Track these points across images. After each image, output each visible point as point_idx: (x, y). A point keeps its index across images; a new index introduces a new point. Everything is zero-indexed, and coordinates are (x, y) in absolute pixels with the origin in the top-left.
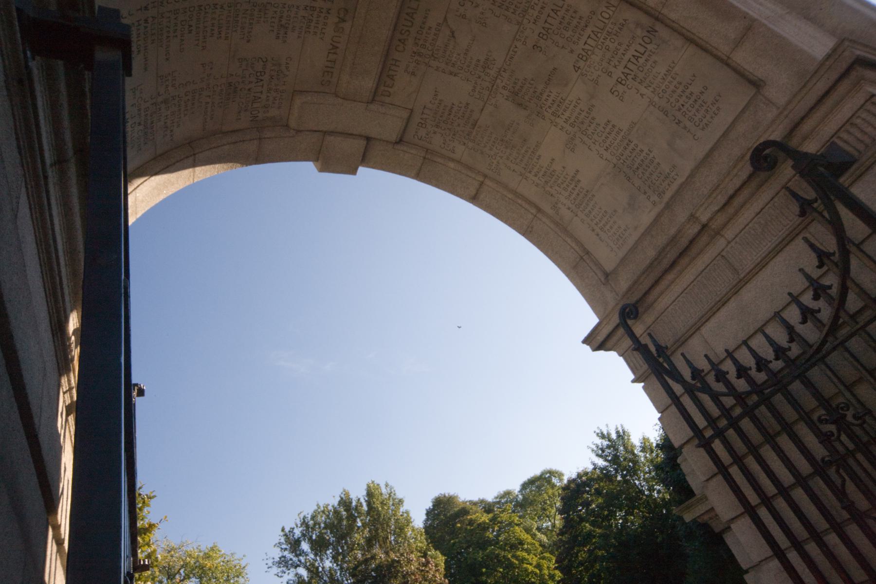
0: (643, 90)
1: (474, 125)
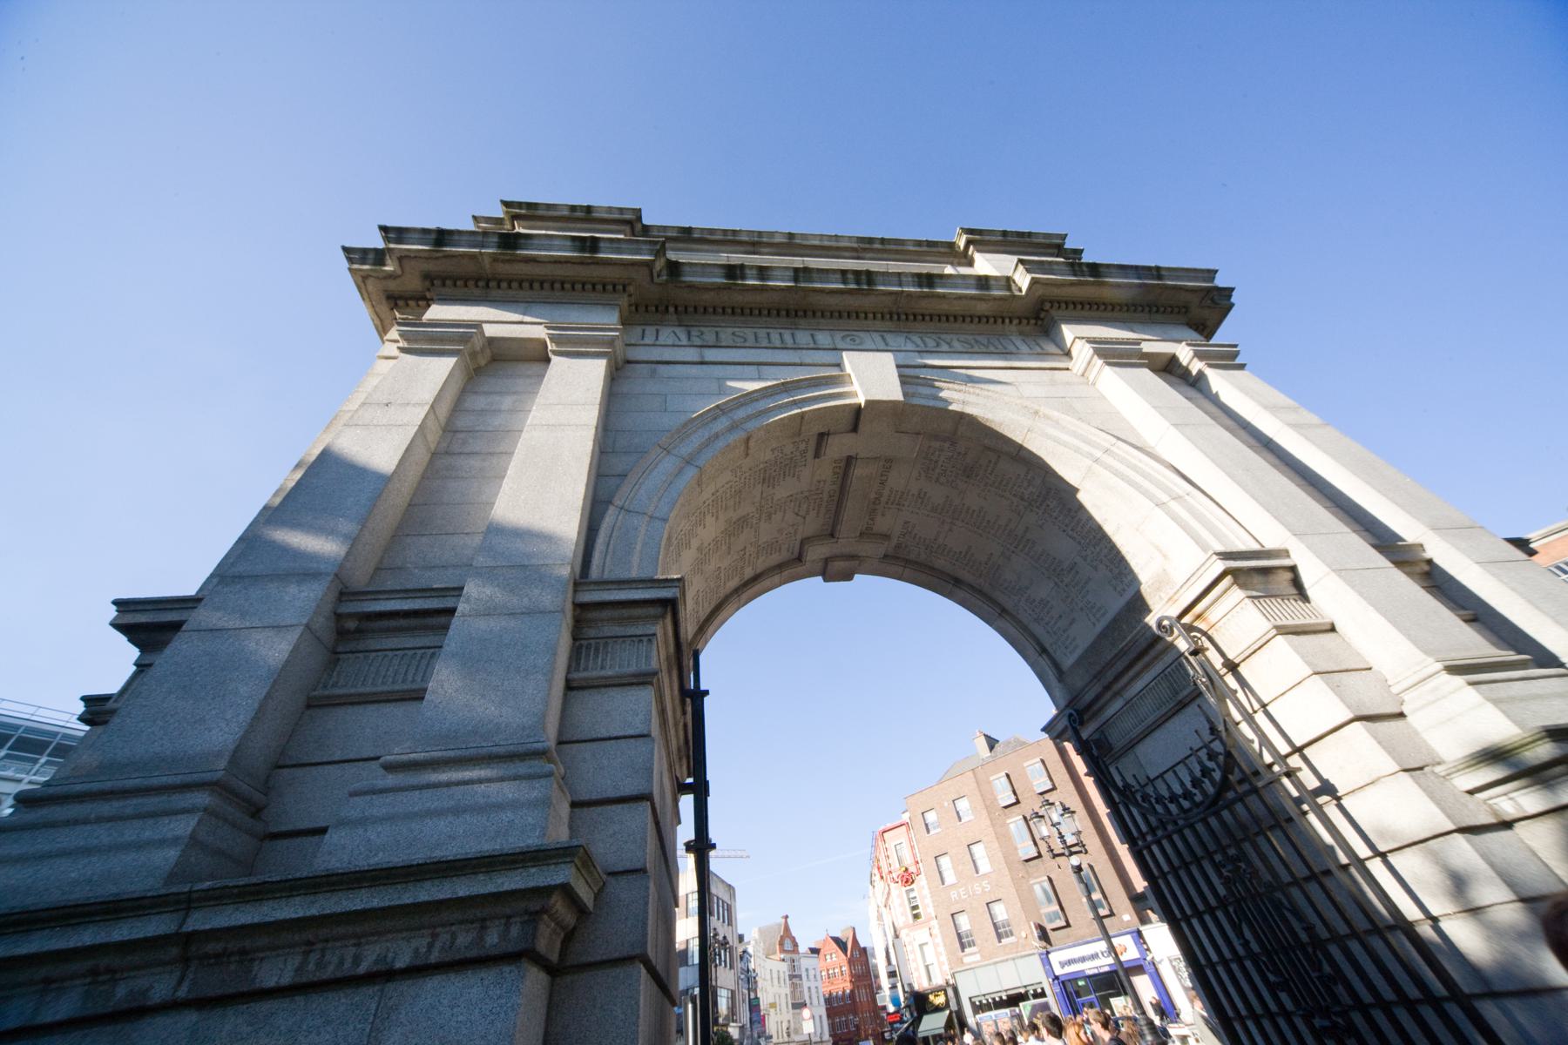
1: (764, 479)
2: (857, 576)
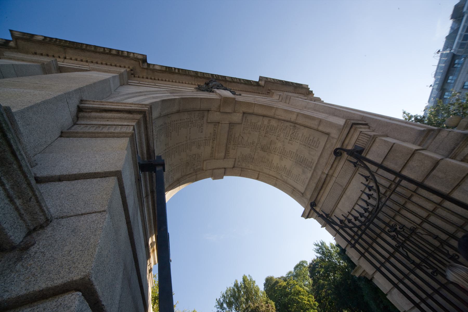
0: (297, 141)
1: (253, 159)
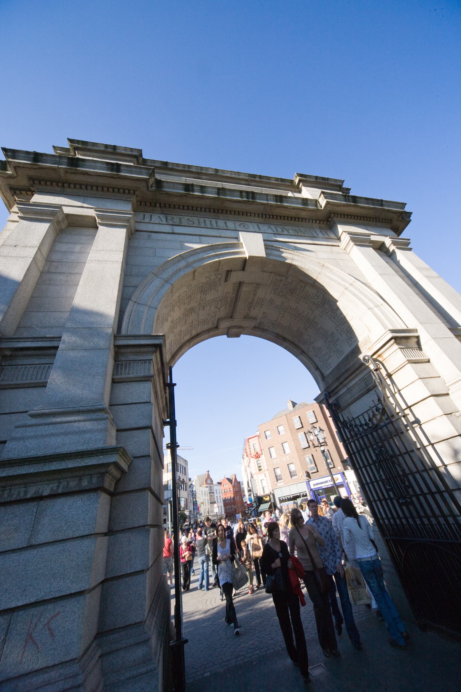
1: (202, 291)
2: (242, 336)
